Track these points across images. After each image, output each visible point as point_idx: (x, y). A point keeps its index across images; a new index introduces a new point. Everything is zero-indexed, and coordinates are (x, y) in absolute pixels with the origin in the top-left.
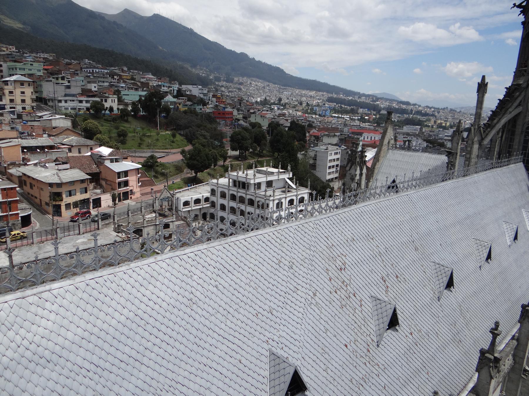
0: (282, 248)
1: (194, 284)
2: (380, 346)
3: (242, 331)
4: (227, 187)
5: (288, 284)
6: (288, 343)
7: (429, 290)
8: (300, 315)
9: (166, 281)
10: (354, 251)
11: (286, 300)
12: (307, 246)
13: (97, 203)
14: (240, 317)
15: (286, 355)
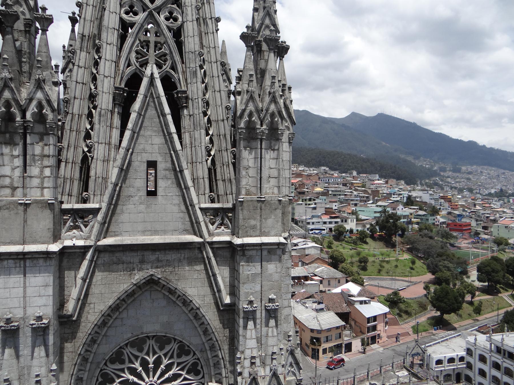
4: (488, 352)
13: (349, 347)
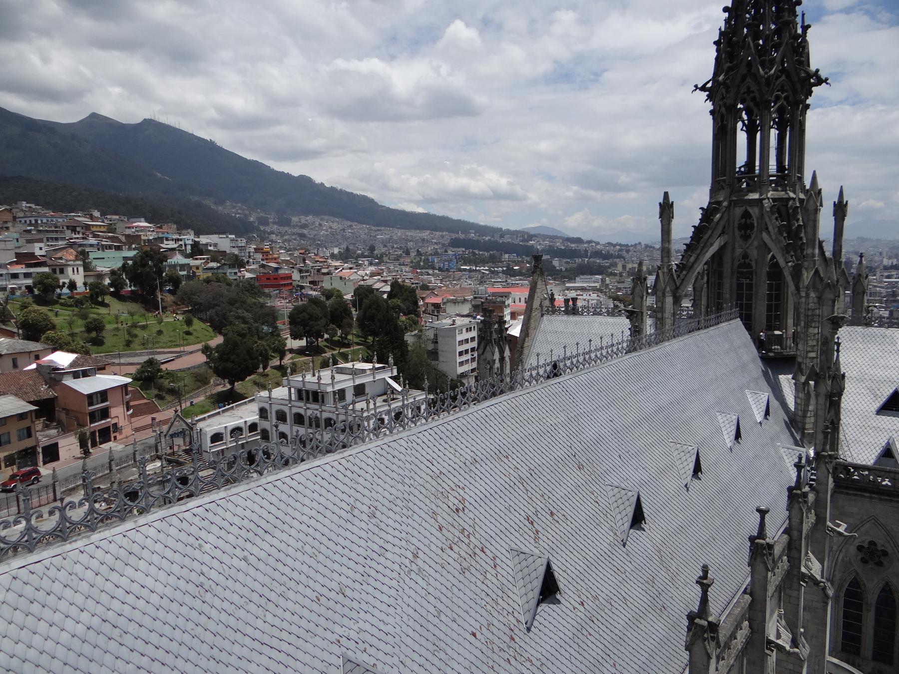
0: (355, 486)
1: (206, 558)
2: (533, 629)
3: (294, 629)
5: (370, 543)
6: (374, 641)
7: (607, 530)
8: (393, 592)
9: (156, 559)
10: (478, 479)
11: (367, 569)
12: (398, 478)
13: (52, 453)
14: (290, 605)
15: (372, 661)
